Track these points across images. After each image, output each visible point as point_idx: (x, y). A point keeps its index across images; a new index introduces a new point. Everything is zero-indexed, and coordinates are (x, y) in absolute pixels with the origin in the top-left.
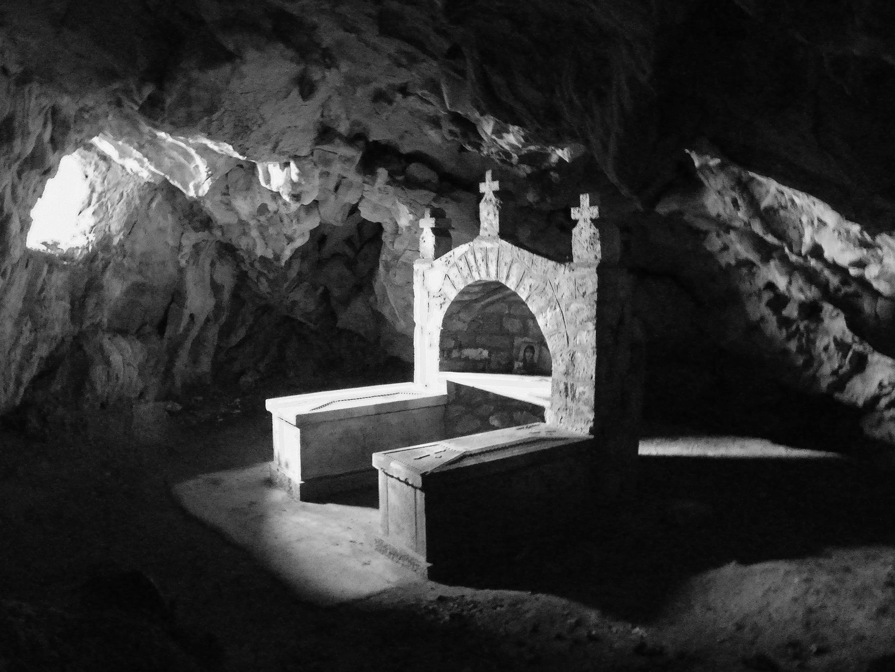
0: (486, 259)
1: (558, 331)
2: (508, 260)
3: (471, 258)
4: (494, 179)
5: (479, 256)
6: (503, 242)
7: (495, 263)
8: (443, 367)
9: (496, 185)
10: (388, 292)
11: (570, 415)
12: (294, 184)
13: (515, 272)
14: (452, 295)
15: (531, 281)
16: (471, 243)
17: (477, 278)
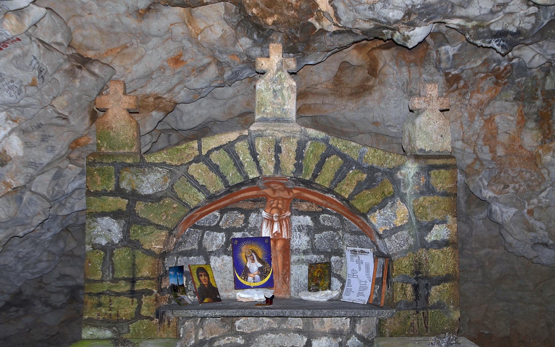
1: (401, 228)
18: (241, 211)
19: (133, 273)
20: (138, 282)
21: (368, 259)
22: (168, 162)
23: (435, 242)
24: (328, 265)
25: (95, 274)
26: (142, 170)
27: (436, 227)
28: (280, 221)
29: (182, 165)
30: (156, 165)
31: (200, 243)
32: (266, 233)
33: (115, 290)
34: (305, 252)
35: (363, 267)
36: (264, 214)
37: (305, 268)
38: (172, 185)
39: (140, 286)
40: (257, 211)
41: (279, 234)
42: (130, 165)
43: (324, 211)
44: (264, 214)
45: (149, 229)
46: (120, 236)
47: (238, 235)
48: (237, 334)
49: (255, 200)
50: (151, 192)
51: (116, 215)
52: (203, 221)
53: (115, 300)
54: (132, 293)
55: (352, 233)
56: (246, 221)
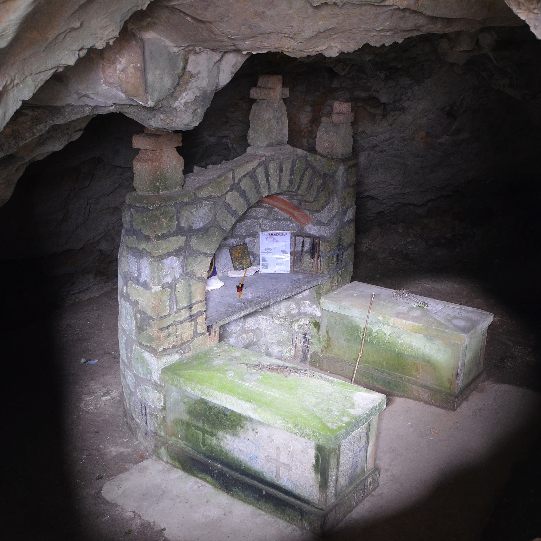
0: (281, 170)
7: (288, 173)
19: (190, 300)
20: (194, 308)
22: (213, 194)
24: (244, 244)
25: (165, 310)
26: (195, 206)
29: (222, 195)
33: (179, 319)
38: (215, 215)
39: (196, 309)
42: (187, 204)
45: (199, 259)
46: (180, 271)
50: (202, 225)
53: (179, 327)
54: (192, 318)
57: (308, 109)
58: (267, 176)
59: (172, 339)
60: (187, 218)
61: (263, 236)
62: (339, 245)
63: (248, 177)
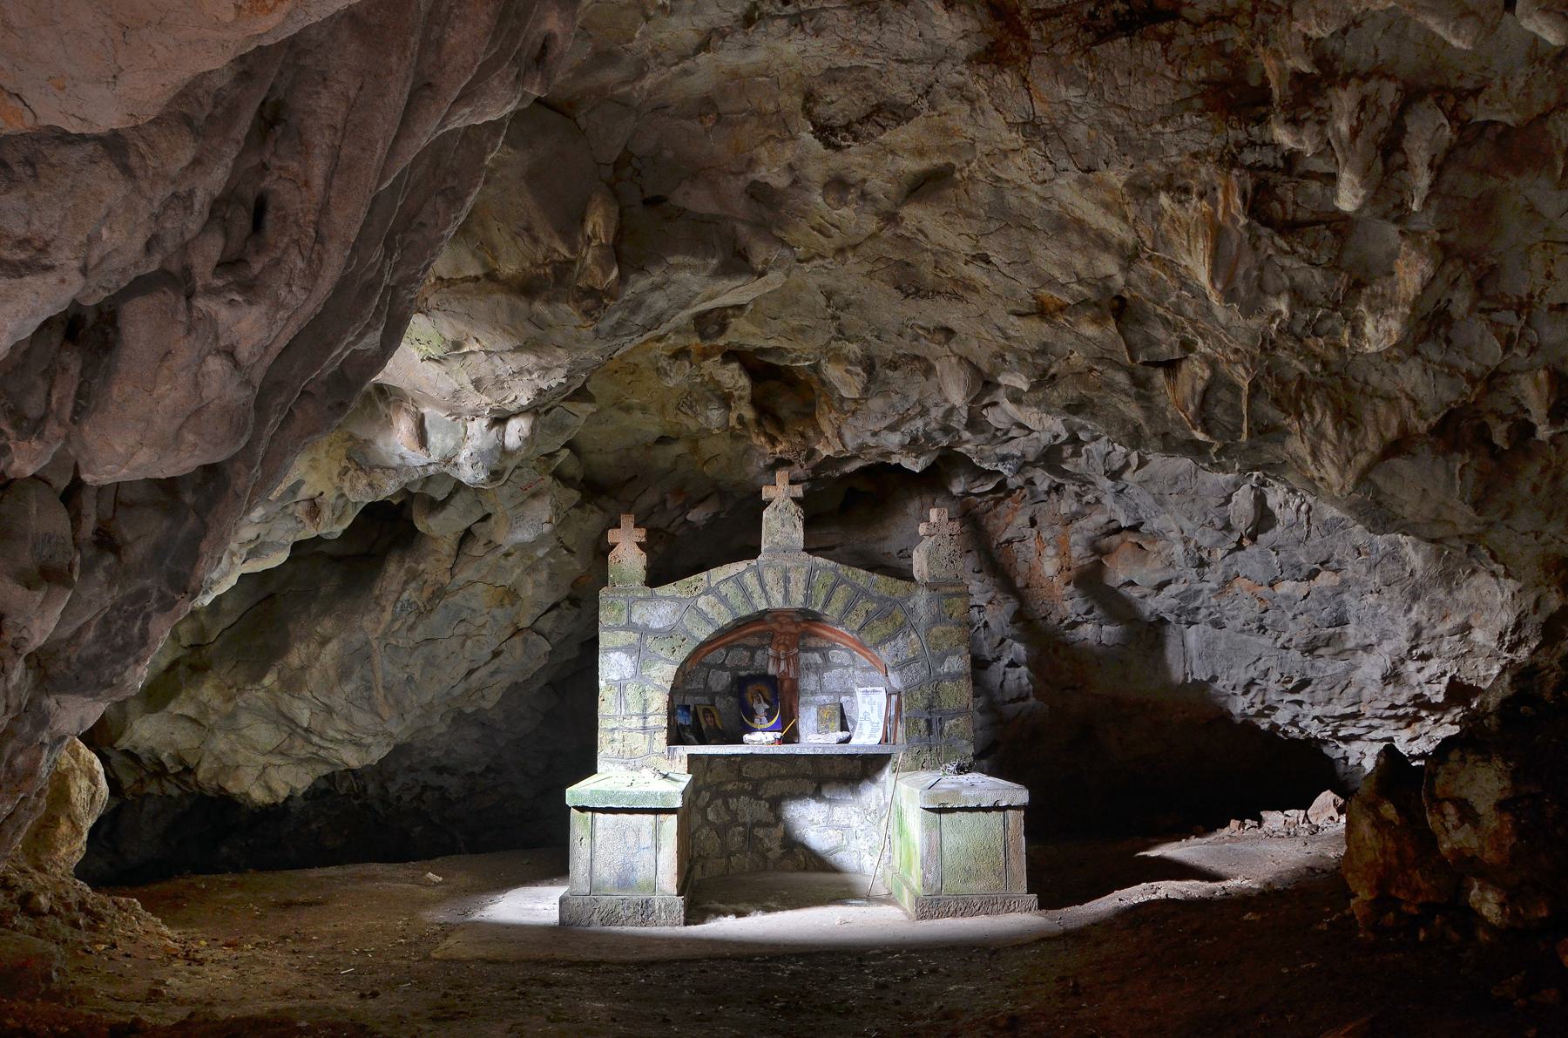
0: (787, 580)
1: (914, 659)
2: (830, 581)
3: (750, 580)
4: (792, 483)
5: (769, 577)
6: (820, 560)
7: (801, 585)
8: (677, 736)
9: (798, 491)
10: (377, 659)
11: (939, 755)
12: (504, 451)
13: (841, 593)
14: (703, 633)
15: (872, 606)
16: (754, 562)
17: (763, 606)
18: (746, 648)
19: (645, 709)
20: (651, 719)
21: (881, 697)
23: (949, 674)
27: (949, 658)
28: (787, 659)
30: (665, 598)
31: (706, 684)
32: (772, 670)
34: (813, 693)
35: (876, 708)
36: (771, 651)
37: (814, 710)
39: (652, 721)
40: (762, 647)
41: (786, 674)
43: (834, 647)
44: (771, 651)
45: (659, 665)
47: (743, 673)
48: (743, 780)
49: (761, 634)
51: (628, 649)
52: (709, 659)
55: (865, 670)
56: (752, 658)
57: (1050, 551)
58: (762, 585)
59: (617, 745)
60: (641, 616)
61: (859, 692)
62: (930, 706)
63: (730, 583)
